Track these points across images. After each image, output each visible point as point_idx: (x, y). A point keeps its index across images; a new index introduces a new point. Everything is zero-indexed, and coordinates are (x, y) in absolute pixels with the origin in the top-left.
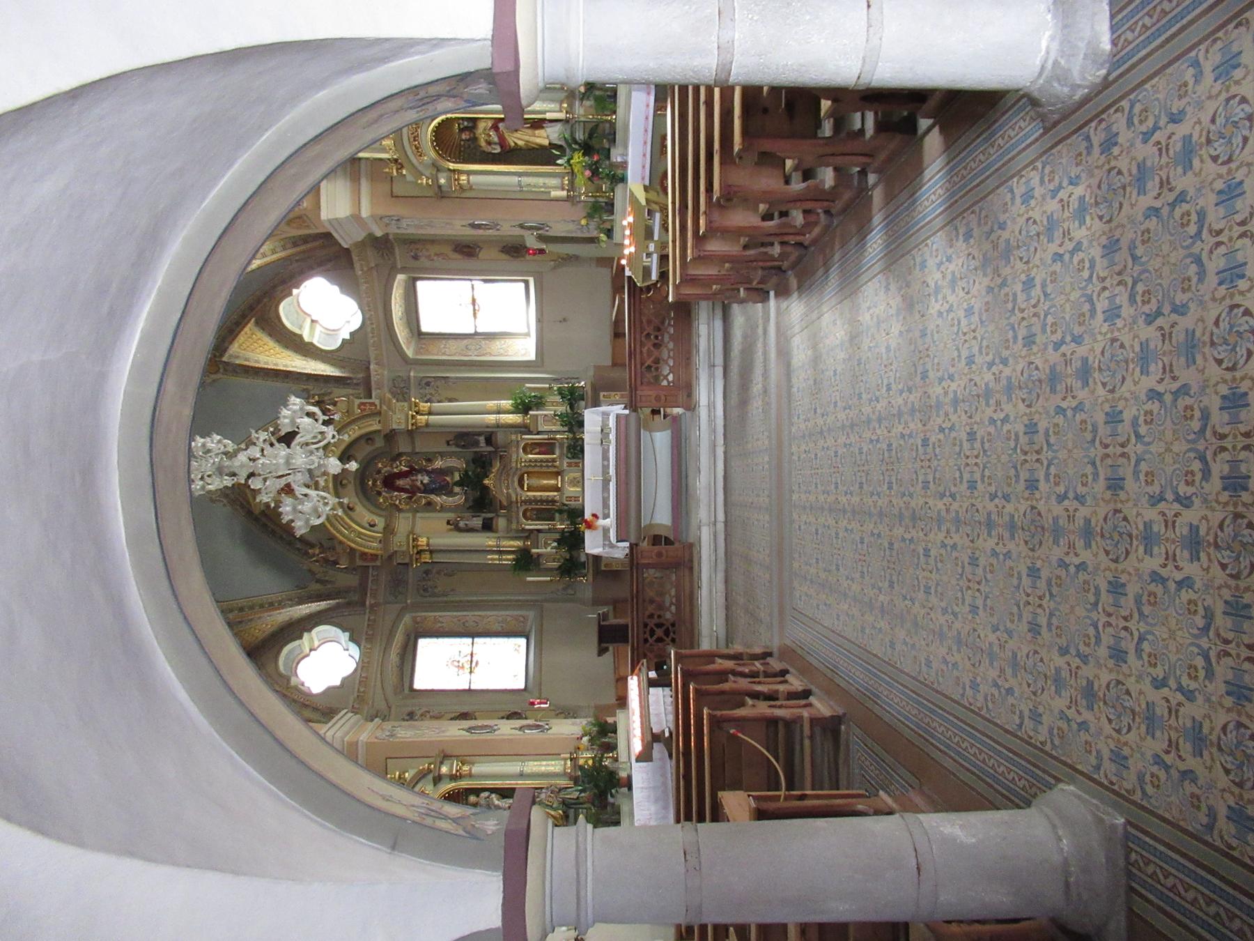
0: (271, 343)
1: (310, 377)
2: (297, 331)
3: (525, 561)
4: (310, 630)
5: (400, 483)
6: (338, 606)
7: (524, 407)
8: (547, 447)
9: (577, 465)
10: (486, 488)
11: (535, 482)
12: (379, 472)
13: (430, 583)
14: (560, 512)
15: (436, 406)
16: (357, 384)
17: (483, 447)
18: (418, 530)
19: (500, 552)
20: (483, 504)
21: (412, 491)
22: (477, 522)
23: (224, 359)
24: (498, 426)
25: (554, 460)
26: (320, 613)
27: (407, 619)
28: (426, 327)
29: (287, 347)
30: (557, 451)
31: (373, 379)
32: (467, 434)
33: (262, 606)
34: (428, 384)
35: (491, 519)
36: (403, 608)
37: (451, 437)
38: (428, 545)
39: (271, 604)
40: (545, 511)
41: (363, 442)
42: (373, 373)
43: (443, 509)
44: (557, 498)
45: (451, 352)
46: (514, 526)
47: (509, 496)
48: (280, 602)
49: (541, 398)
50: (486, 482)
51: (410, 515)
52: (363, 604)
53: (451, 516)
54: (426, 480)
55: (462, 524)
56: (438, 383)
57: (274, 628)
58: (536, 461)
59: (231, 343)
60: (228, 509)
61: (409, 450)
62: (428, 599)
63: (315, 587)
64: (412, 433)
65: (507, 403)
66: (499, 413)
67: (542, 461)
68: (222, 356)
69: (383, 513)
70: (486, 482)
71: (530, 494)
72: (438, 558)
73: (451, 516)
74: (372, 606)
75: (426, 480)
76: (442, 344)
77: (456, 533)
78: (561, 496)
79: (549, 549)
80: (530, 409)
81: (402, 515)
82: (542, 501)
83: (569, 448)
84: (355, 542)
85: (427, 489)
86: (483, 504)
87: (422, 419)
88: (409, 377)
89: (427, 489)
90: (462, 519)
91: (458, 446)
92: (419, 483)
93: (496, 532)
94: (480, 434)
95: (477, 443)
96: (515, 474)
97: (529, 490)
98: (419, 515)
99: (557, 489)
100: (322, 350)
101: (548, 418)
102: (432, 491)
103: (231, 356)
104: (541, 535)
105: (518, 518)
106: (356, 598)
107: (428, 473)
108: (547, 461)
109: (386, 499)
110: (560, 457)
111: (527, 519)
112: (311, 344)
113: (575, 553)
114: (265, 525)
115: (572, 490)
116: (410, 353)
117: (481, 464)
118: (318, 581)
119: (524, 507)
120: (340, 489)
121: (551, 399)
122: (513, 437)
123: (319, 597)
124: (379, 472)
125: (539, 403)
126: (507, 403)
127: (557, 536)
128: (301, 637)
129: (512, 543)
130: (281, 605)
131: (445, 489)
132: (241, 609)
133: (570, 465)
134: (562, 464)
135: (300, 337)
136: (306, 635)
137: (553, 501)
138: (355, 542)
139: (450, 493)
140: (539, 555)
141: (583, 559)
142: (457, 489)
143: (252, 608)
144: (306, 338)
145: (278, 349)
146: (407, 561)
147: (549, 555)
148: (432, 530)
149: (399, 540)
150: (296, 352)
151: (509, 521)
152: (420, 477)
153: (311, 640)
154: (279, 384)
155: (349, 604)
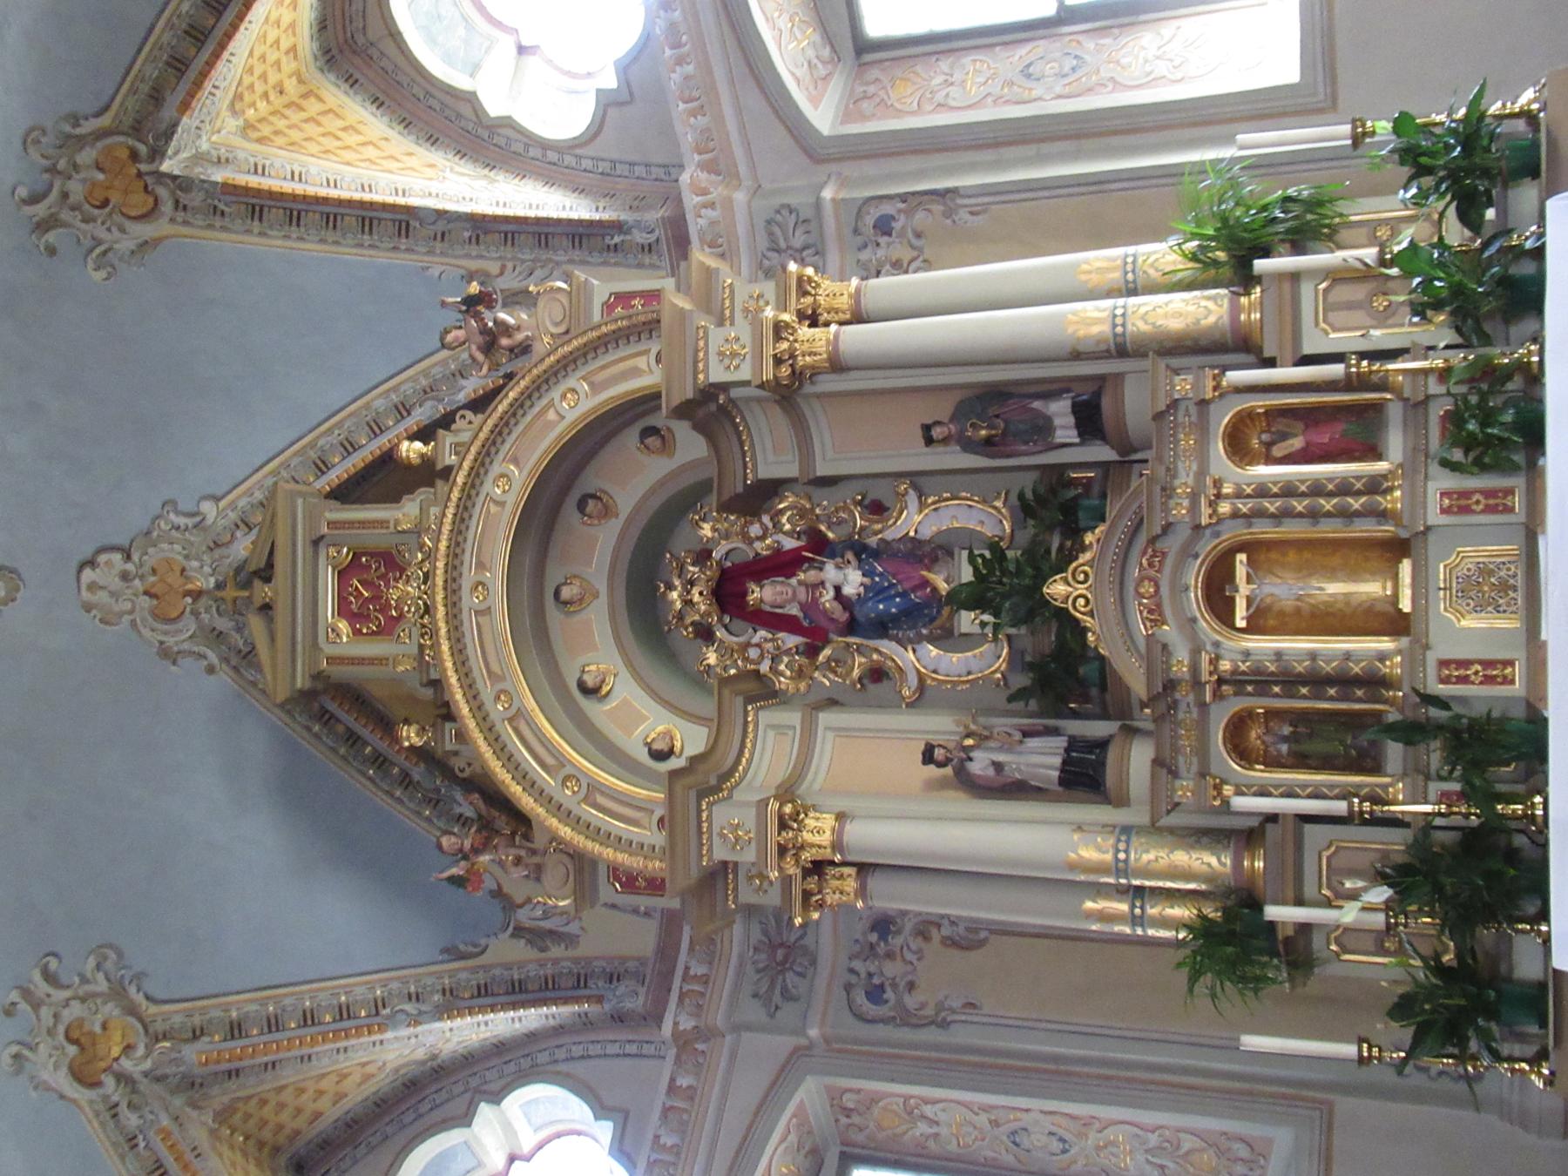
0: (375, 124)
1: (482, 228)
2: (461, 81)
3: (1239, 945)
4: (496, 1098)
5: (762, 594)
6: (586, 1023)
7: (1236, 253)
8: (1343, 419)
9: (1496, 502)
10: (1063, 617)
11: (1283, 589)
12: (703, 556)
13: (891, 969)
14: (1411, 732)
15: (886, 288)
16: (649, 248)
17: (1068, 446)
18: (817, 779)
19: (1139, 891)
20: (1062, 676)
21: (814, 634)
22: (1042, 758)
23: (166, 166)
24: (1122, 348)
25: (1375, 486)
26: (532, 1037)
27: (808, 1093)
28: (876, 25)
29: (433, 141)
30: (1395, 443)
31: (694, 227)
32: (995, 395)
33: (309, 1019)
34: (884, 227)
35: (1102, 745)
36: (796, 1051)
37: (943, 409)
38: (837, 845)
39: (344, 1013)
40: (1334, 725)
41: (631, 436)
42: (691, 201)
43: (923, 696)
44: (1394, 667)
45: (970, 95)
46: (1184, 789)
47: (1158, 652)
48: (377, 1006)
49: (1314, 204)
50: (1057, 589)
51: (793, 718)
52: (659, 1020)
53: (941, 726)
54: (853, 581)
55: (980, 764)
56: (920, 215)
57: (370, 1088)
58: (1289, 490)
59: (185, 106)
60: (224, 677)
61: (792, 470)
62: (882, 1031)
63: (507, 952)
64: (790, 390)
65: (1162, 255)
66: (1132, 291)
67: (1317, 489)
68: (157, 154)
69: (708, 707)
70: (1057, 589)
71: (1262, 644)
72: (890, 896)
73: (941, 726)
74: (683, 1042)
75: (853, 581)
76: (936, 74)
77: (960, 803)
78: (1414, 657)
79: (1349, 914)
80: (1266, 253)
81: (766, 717)
82: (1317, 681)
83: (1454, 419)
84: (577, 822)
85: (859, 621)
86: (1062, 676)
87: (813, 341)
88: (818, 205)
89: (859, 621)
90: (983, 739)
91: (969, 446)
92: (828, 596)
93: (1122, 801)
94: (1052, 389)
95: (1042, 429)
96: (1188, 553)
97: (1254, 627)
98: (825, 718)
99: (1395, 623)
100: (545, 145)
101: (1349, 317)
102: (881, 628)
103: (199, 158)
104: (1309, 828)
105: (1203, 752)
106: (636, 1001)
107: (862, 552)
108: (1344, 488)
109: (725, 651)
110: (1411, 469)
111: (1244, 755)
112: (508, 123)
113: (1486, 935)
114: (353, 739)
115: (1467, 629)
116: (823, 117)
117: (1060, 512)
118: (519, 931)
119: (1237, 705)
120: (553, 614)
121: (1361, 210)
122: (1183, 385)
123: (517, 993)
124: (703, 556)
125: (1308, 226)
126: (1162, 255)
127: (1395, 842)
128: (465, 1119)
129: (1181, 857)
130: (379, 1014)
131: (920, 617)
132: (236, 1029)
133: (1459, 504)
134: (1416, 499)
135: (471, 98)
136: (485, 1110)
137: (1374, 682)
138: (577, 822)
139: (947, 637)
140: (1305, 928)
141: (1526, 968)
142: (967, 621)
143: (273, 1024)
144: (494, 107)
145: (399, 143)
146: (773, 898)
147: (1347, 937)
148: (875, 782)
149: (733, 825)
150: (462, 154)
151: (1164, 765)
152: (830, 572)
153: (507, 1127)
154: (382, 258)
155: (619, 1018)
